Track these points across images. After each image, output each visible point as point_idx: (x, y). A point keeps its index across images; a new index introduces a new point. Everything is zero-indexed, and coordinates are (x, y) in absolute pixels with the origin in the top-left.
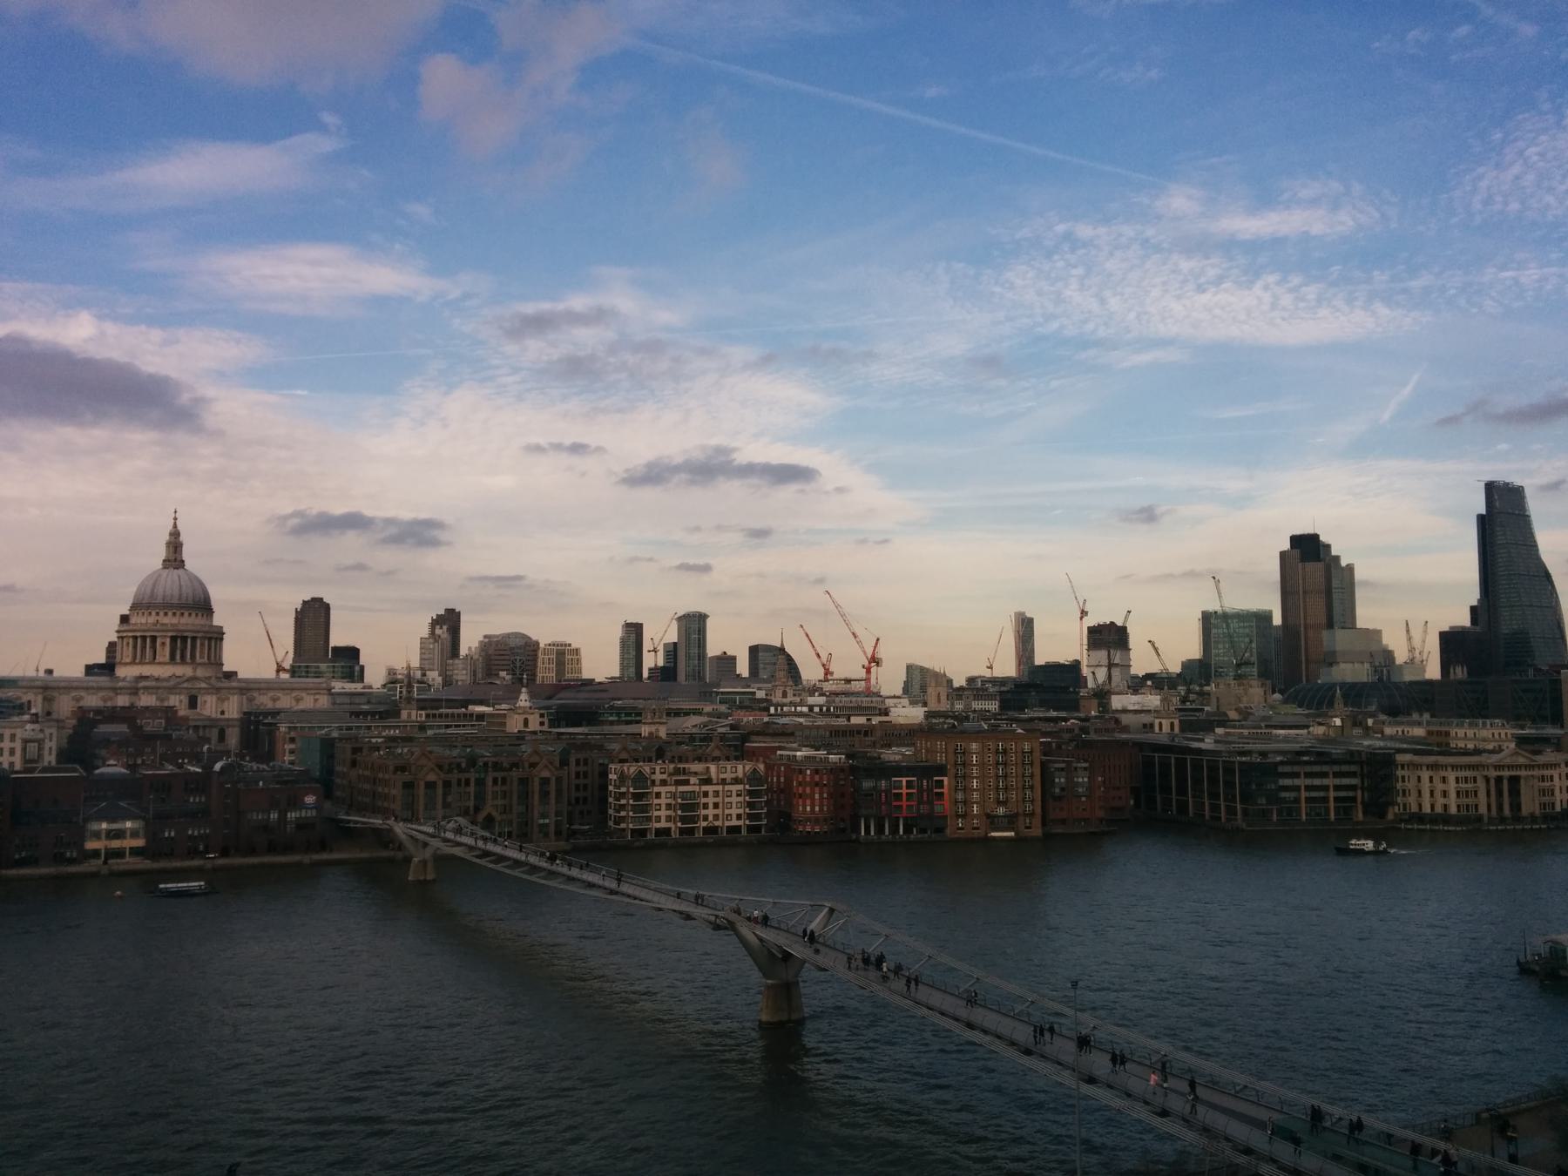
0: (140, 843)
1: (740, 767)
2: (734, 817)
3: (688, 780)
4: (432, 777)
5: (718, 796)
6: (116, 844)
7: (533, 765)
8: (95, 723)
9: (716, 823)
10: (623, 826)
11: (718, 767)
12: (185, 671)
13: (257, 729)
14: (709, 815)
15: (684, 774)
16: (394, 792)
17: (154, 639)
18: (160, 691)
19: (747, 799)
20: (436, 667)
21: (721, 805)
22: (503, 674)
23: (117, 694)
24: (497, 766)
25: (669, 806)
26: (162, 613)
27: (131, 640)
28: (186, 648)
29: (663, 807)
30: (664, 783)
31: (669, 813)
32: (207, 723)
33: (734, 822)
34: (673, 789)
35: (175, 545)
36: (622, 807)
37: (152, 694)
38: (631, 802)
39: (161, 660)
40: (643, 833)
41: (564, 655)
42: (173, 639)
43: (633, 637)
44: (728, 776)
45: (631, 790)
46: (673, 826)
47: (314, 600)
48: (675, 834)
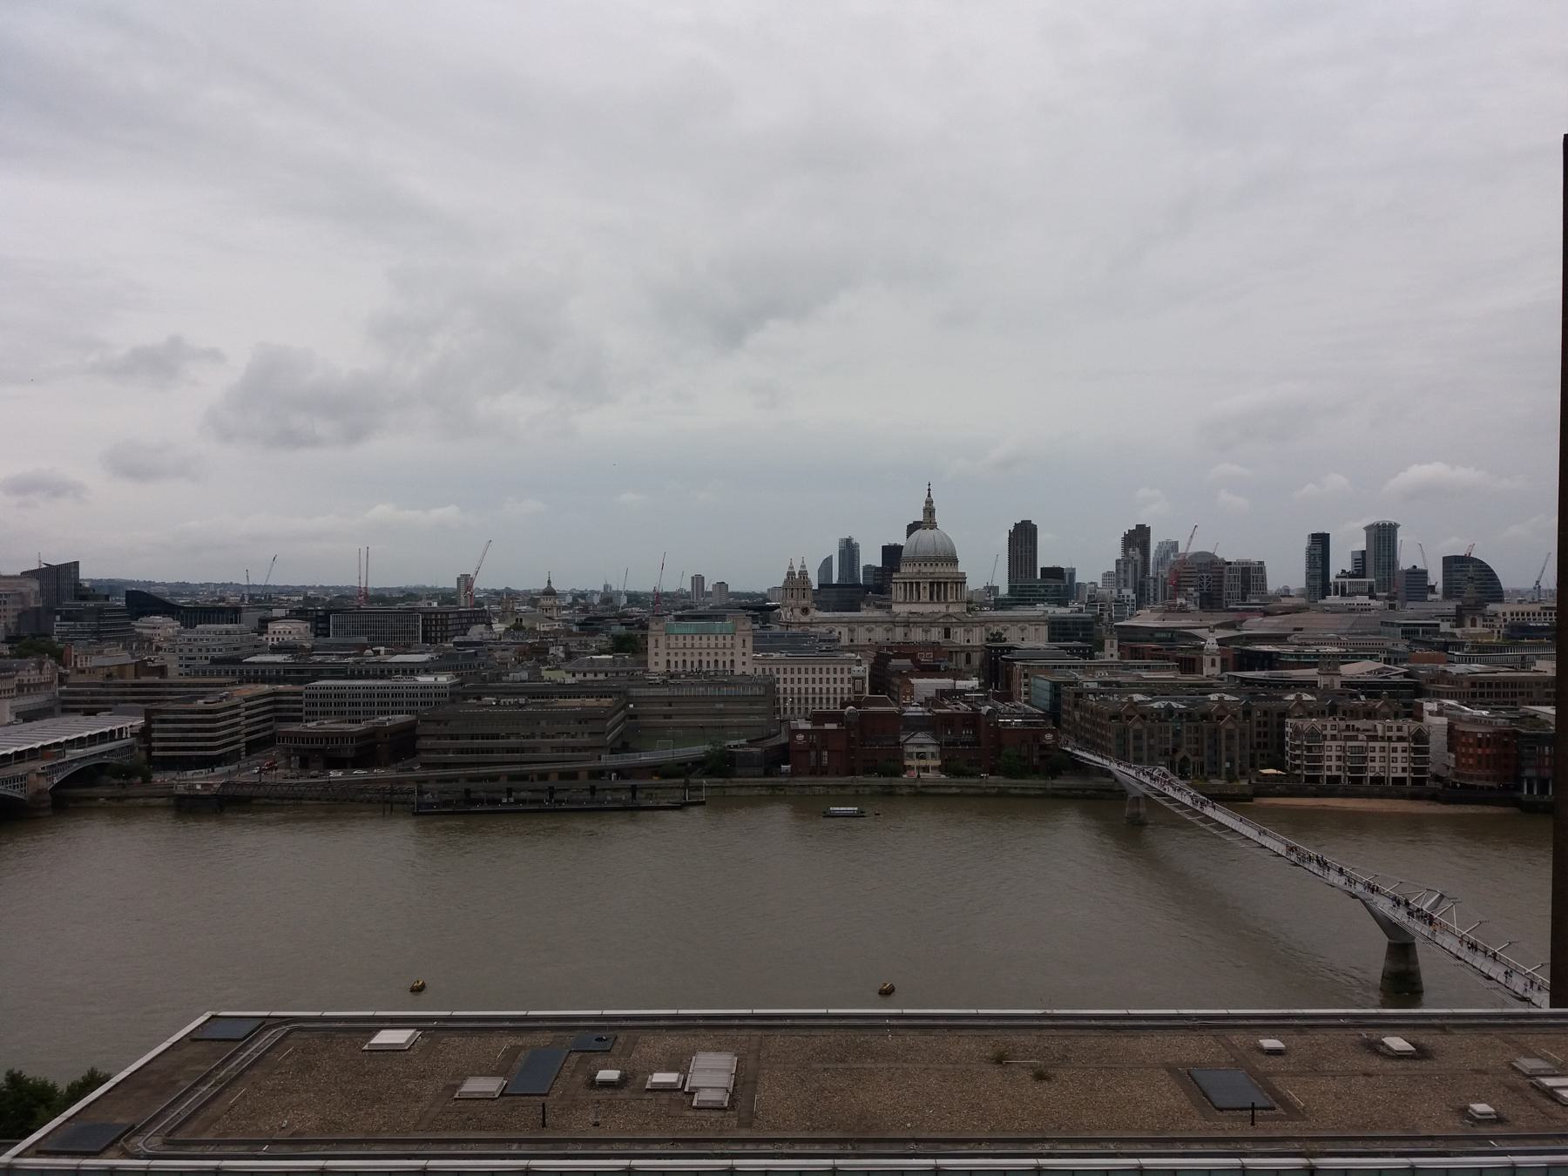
0: (938, 763)
1: (1405, 728)
2: (1400, 770)
3: (1357, 736)
4: (1138, 726)
5: (1384, 751)
6: (923, 763)
7: (1221, 718)
8: (889, 658)
9: (1382, 774)
10: (1298, 772)
11: (1384, 726)
12: (942, 608)
13: (996, 662)
14: (1375, 768)
15: (1353, 730)
16: (1109, 735)
17: (918, 584)
18: (925, 625)
19: (1412, 755)
20: (1130, 583)
21: (1387, 760)
22: (1191, 589)
23: (895, 626)
24: (1189, 715)
25: (1339, 758)
26: (922, 564)
27: (902, 585)
28: (940, 590)
29: (1334, 758)
30: (1334, 738)
31: (1339, 763)
32: (958, 649)
33: (1400, 774)
34: (1342, 743)
35: (929, 511)
36: (1298, 757)
37: (919, 627)
38: (1305, 753)
39: (925, 600)
40: (1314, 779)
41: (1251, 575)
42: (932, 584)
43: (1319, 547)
44: (1394, 734)
45: (1305, 743)
46: (1343, 774)
47: (1023, 522)
48: (1345, 782)
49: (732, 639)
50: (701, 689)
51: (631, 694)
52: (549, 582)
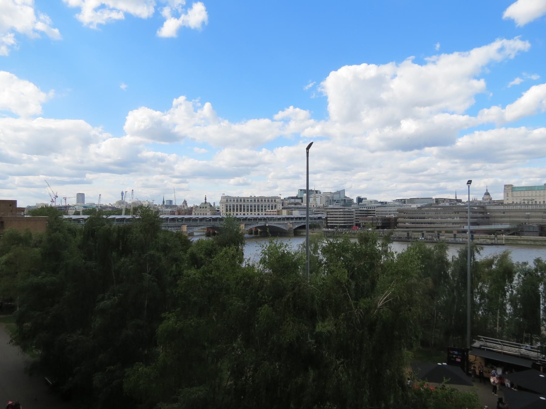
49: (544, 192)
50: (518, 207)
51: (487, 209)
52: (487, 190)
